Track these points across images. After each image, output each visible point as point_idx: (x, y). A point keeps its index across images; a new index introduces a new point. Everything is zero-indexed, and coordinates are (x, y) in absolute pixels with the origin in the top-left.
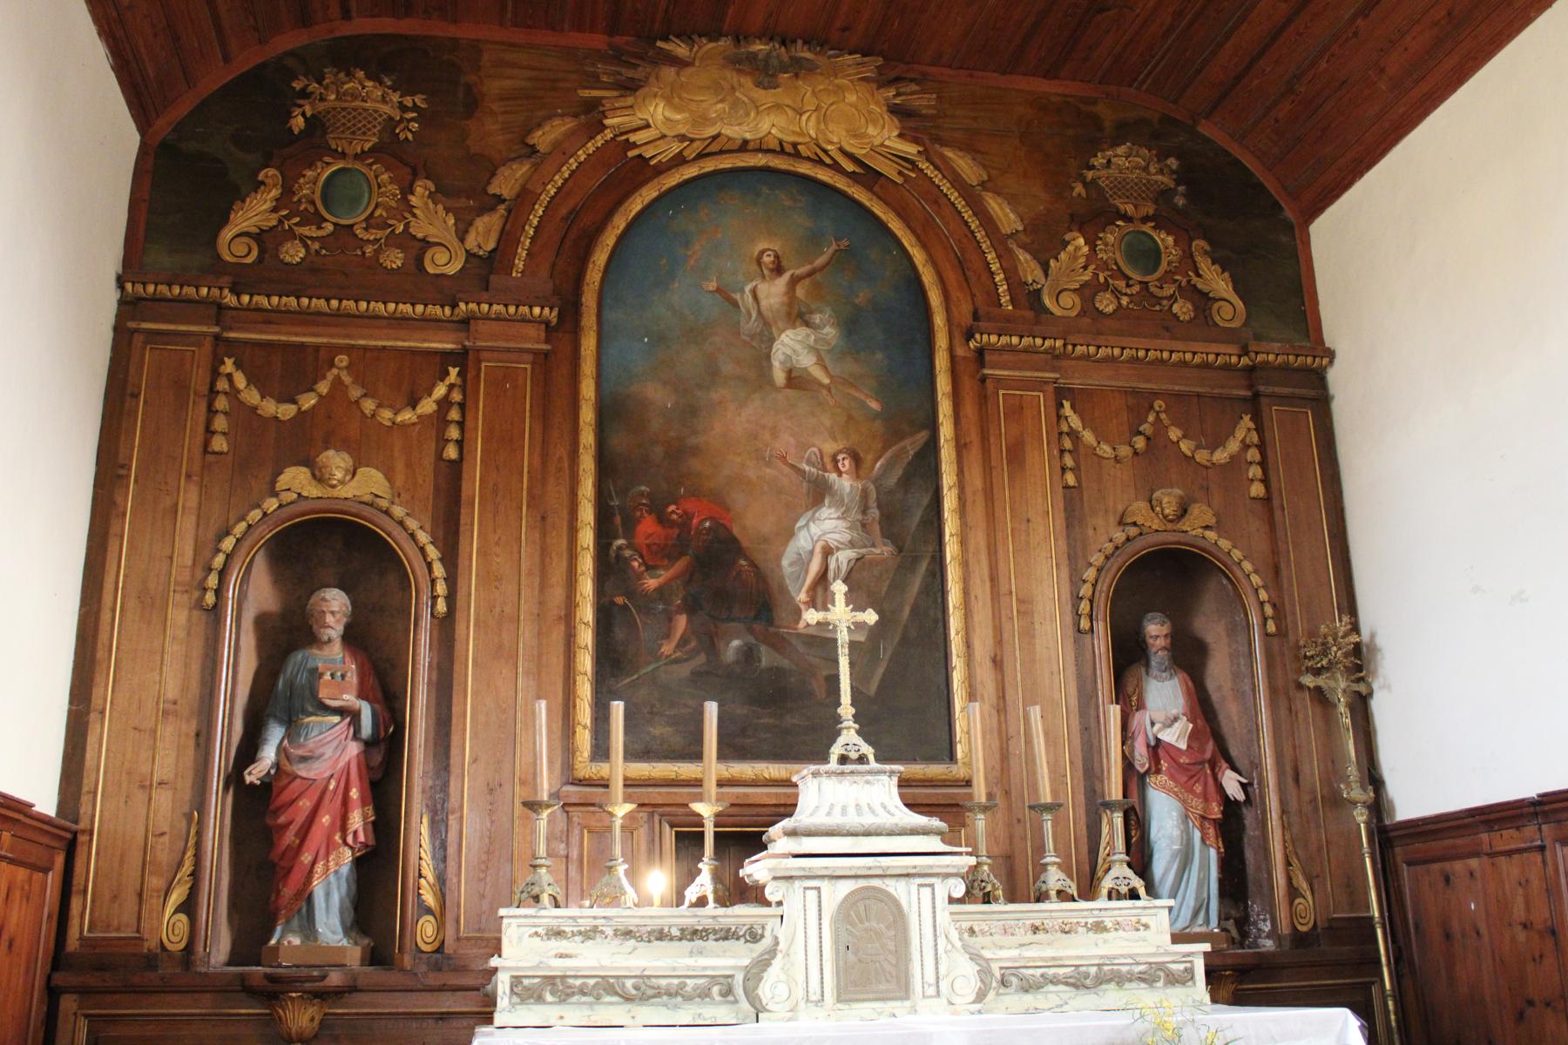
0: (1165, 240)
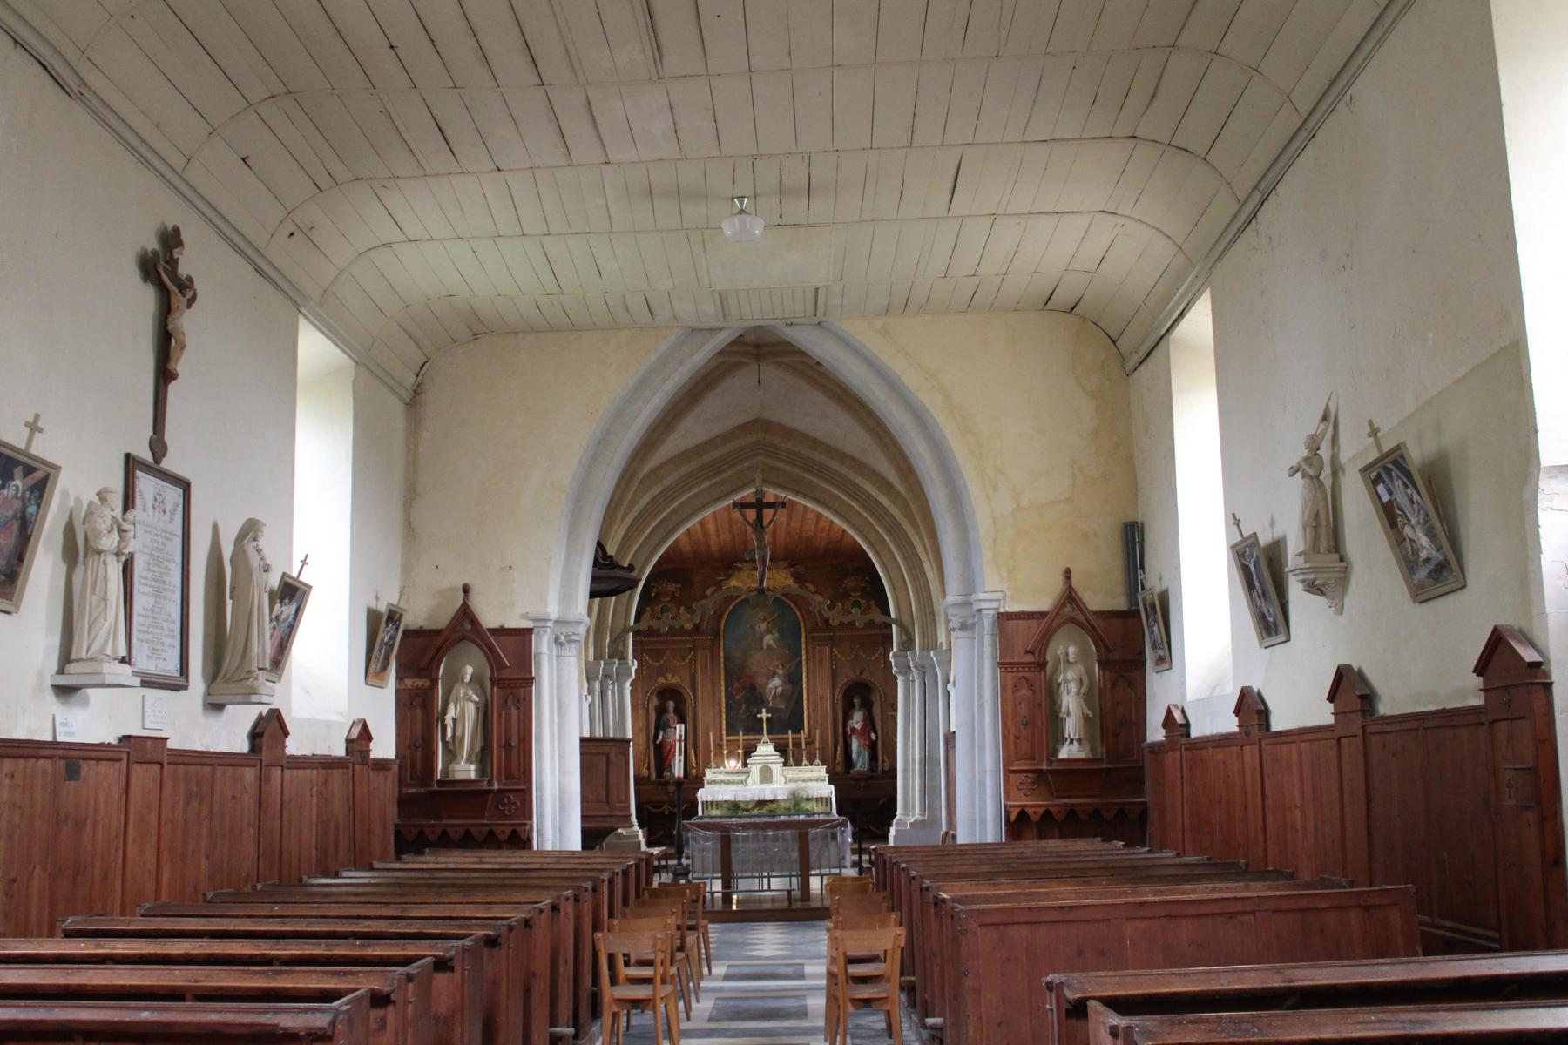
0: (863, 602)
